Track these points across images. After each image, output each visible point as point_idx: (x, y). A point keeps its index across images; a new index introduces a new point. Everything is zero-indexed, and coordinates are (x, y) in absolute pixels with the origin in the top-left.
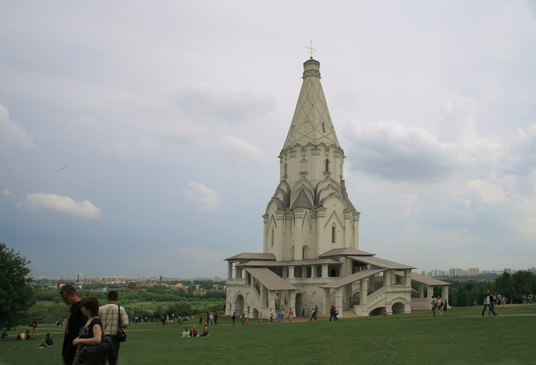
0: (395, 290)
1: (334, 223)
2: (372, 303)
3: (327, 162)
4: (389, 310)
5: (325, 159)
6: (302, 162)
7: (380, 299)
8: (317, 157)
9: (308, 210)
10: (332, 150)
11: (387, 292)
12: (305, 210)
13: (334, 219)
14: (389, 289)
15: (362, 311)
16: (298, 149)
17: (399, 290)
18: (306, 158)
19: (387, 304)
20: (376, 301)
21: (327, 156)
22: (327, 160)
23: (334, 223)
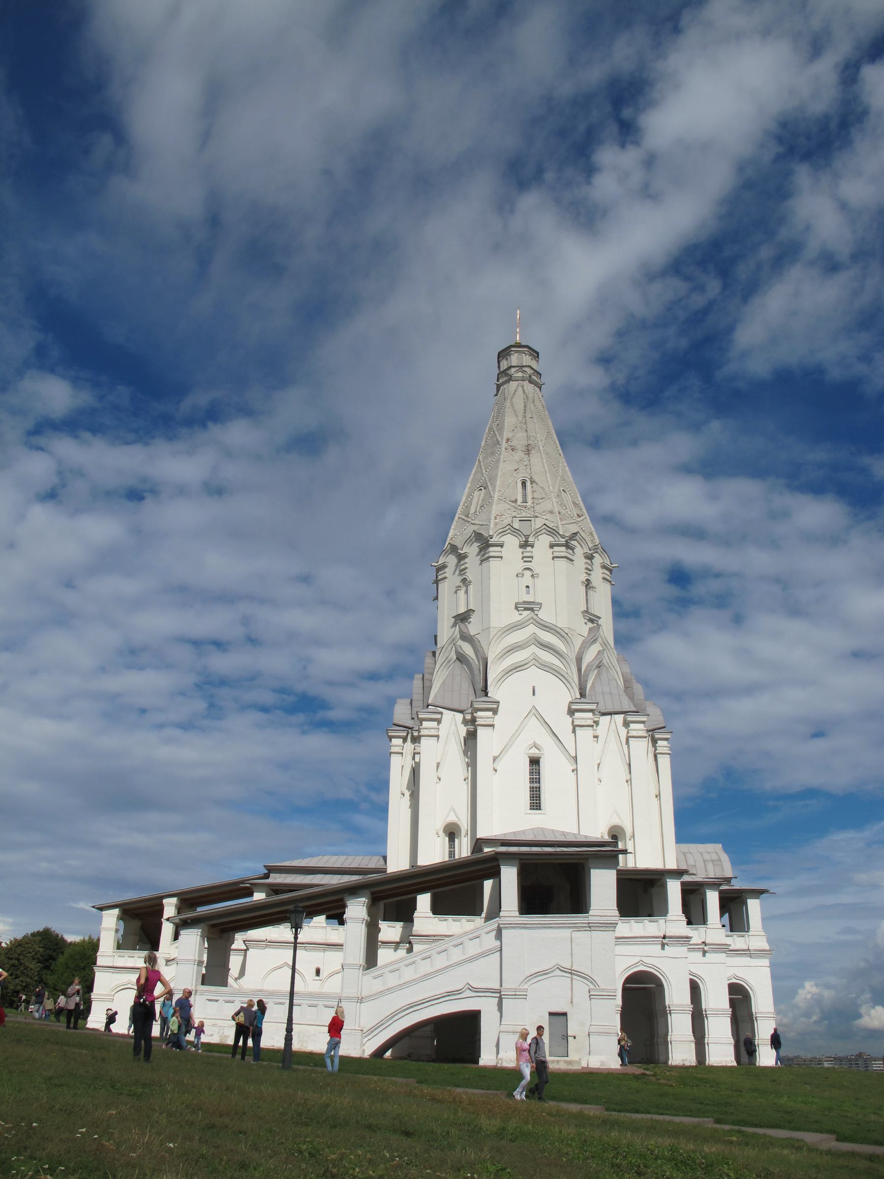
8: (493, 564)
9: (459, 717)
12: (447, 715)
13: (535, 733)
18: (469, 576)
21: (527, 559)
23: (535, 746)
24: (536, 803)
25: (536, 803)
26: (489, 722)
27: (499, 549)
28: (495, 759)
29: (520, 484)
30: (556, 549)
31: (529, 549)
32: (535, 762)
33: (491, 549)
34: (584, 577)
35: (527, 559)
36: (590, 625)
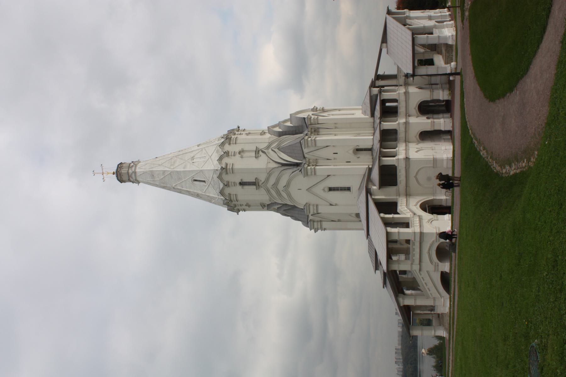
0: (417, 256)
1: (324, 190)
2: (433, 290)
3: (242, 184)
4: (446, 267)
5: (240, 187)
6: (249, 206)
7: (427, 279)
8: (239, 198)
10: (226, 178)
11: (420, 270)
13: (318, 190)
14: (416, 267)
15: (443, 304)
16: (236, 208)
17: (417, 250)
19: (436, 269)
20: (430, 285)
22: (242, 184)
23: (324, 190)
24: (349, 189)
25: (349, 189)
26: (315, 208)
27: (232, 196)
28: (331, 205)
29: (196, 182)
30: (228, 172)
31: (230, 183)
32: (331, 189)
33: (232, 198)
34: (238, 156)
35: (235, 184)
36: (261, 153)
